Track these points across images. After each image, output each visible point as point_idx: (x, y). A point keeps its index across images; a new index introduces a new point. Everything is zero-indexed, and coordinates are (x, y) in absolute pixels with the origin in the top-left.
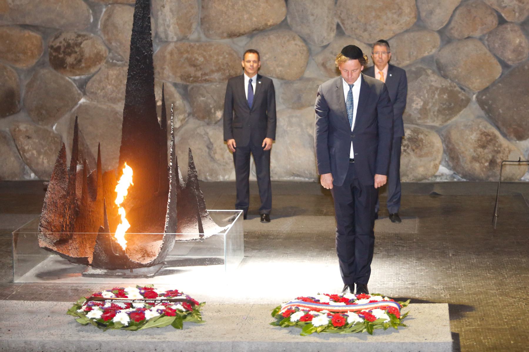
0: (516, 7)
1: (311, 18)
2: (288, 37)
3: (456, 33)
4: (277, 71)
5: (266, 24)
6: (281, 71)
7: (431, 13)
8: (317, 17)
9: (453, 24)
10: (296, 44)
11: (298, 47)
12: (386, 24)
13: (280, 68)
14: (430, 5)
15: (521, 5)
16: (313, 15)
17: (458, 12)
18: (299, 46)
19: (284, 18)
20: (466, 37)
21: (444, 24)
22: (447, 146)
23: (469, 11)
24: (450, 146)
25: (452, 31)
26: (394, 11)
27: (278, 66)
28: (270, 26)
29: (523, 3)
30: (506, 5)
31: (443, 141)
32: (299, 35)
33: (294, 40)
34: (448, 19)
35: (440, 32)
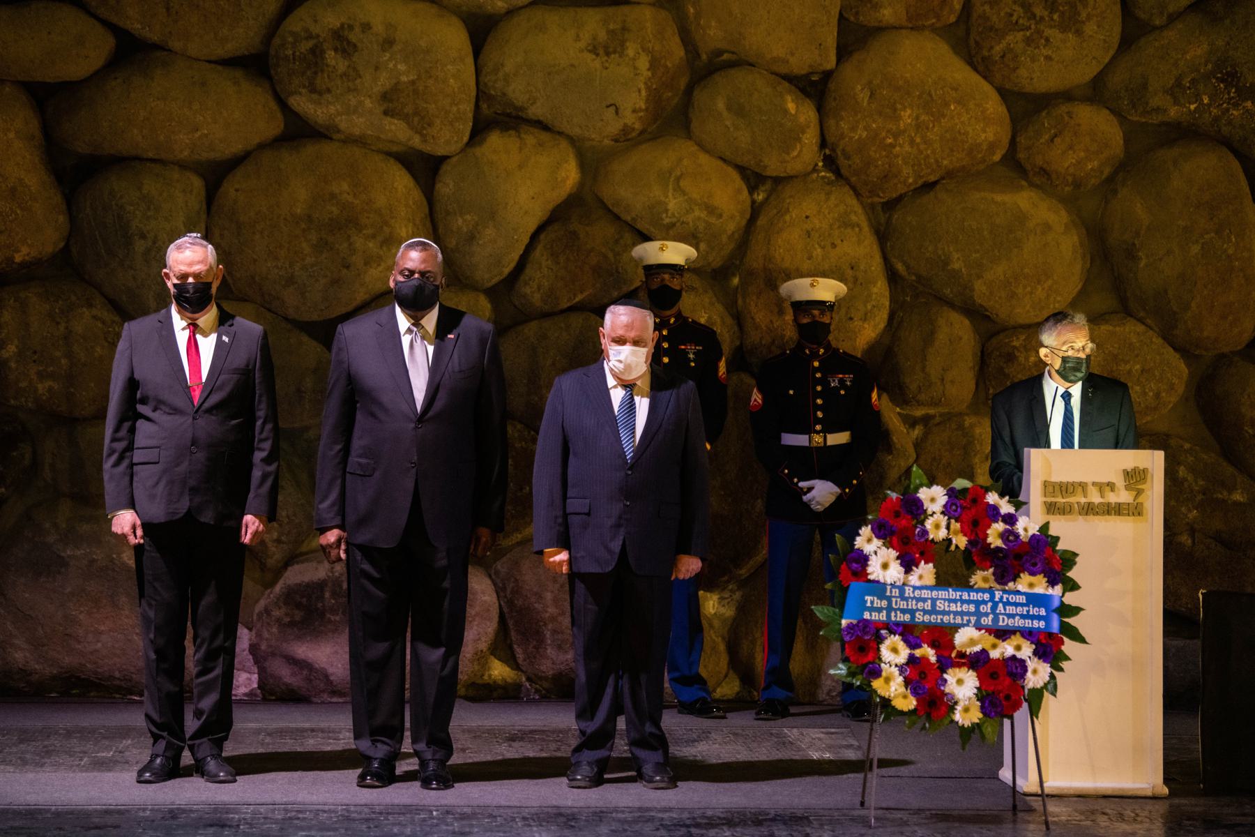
0: (701, 226)
1: (140, 246)
2: (73, 298)
3: (537, 296)
4: (40, 392)
5: (10, 260)
6: (50, 389)
7: (471, 238)
8: (154, 243)
9: (529, 271)
10: (95, 317)
11: (100, 325)
12: (348, 267)
13: (48, 383)
14: (468, 217)
15: (713, 220)
16: (143, 236)
17: (542, 236)
18: (104, 323)
19: (62, 245)
20: (565, 304)
21: (507, 271)
22: (511, 603)
23: (574, 235)
24: (519, 603)
25: (528, 290)
26: (369, 231)
27: (42, 376)
28: (24, 265)
29: (720, 216)
30: (674, 220)
31: (499, 591)
32: (103, 294)
33: (90, 306)
34: (515, 256)
35: (493, 293)
